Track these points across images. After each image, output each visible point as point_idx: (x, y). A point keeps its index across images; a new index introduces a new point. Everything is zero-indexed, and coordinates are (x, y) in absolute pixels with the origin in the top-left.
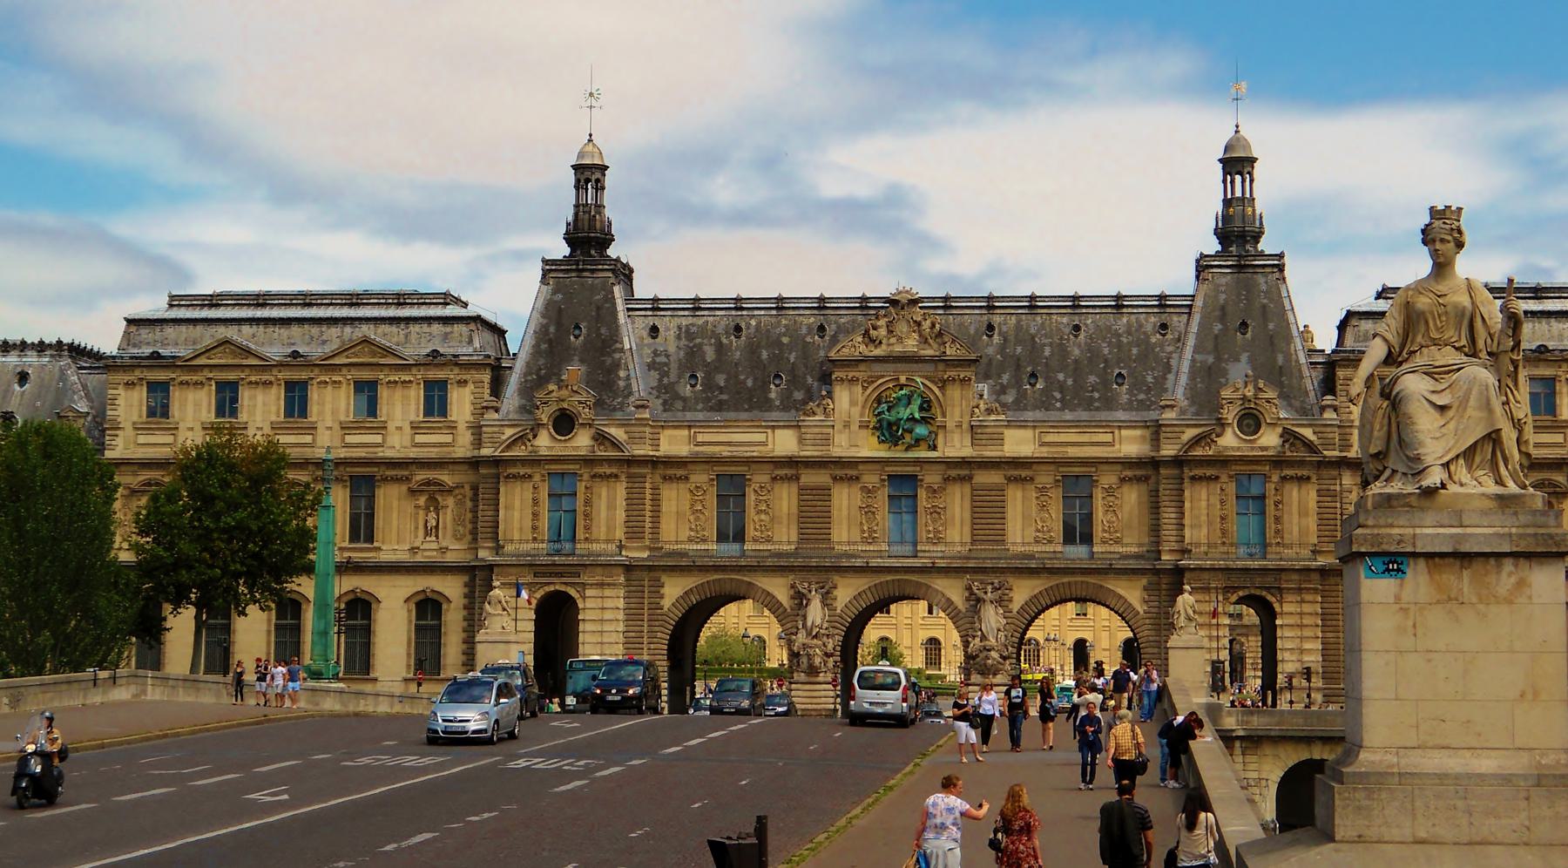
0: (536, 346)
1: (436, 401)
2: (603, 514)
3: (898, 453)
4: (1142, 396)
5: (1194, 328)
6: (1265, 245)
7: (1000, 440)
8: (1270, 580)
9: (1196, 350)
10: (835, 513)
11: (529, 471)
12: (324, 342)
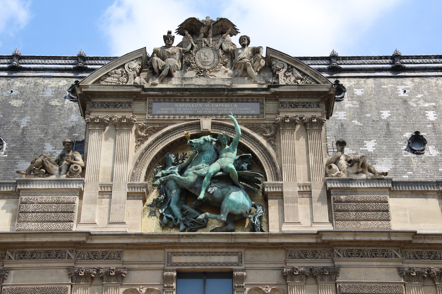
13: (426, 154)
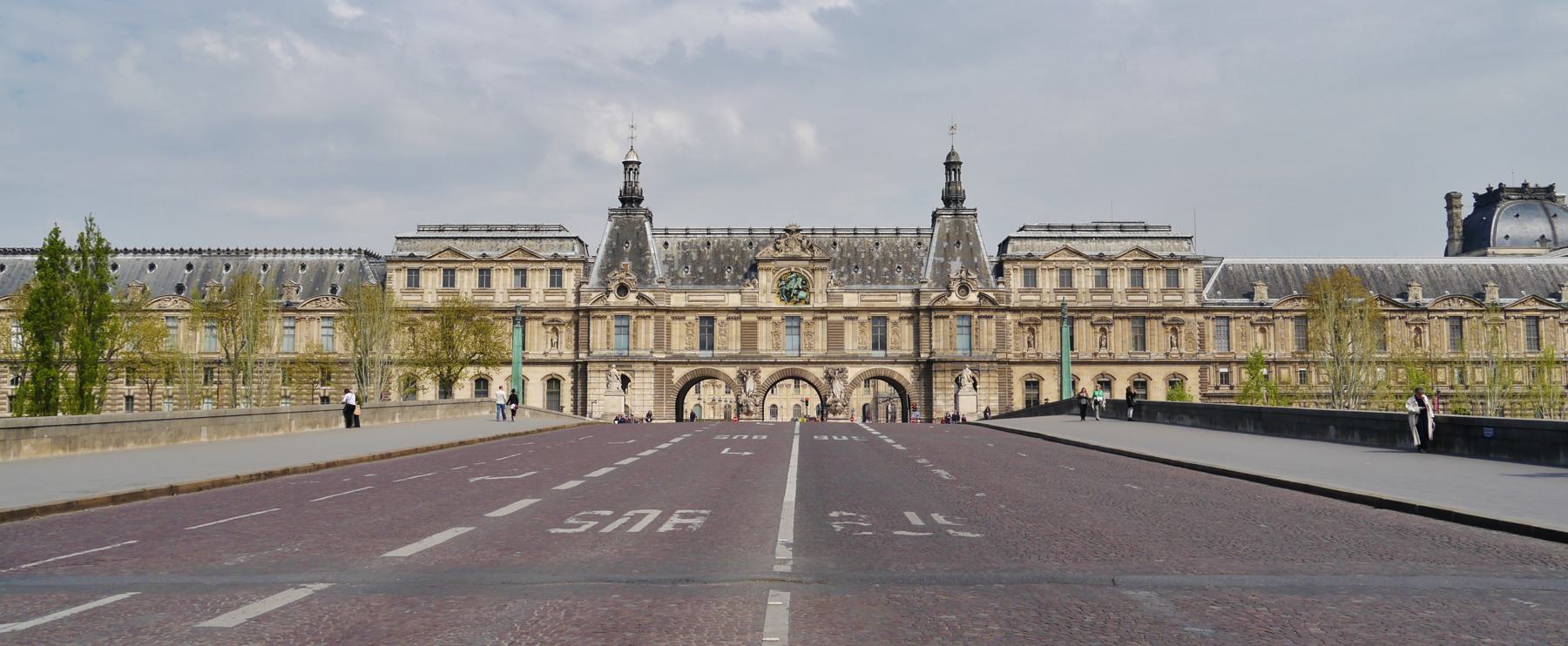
1: (556, 279)
3: (790, 305)
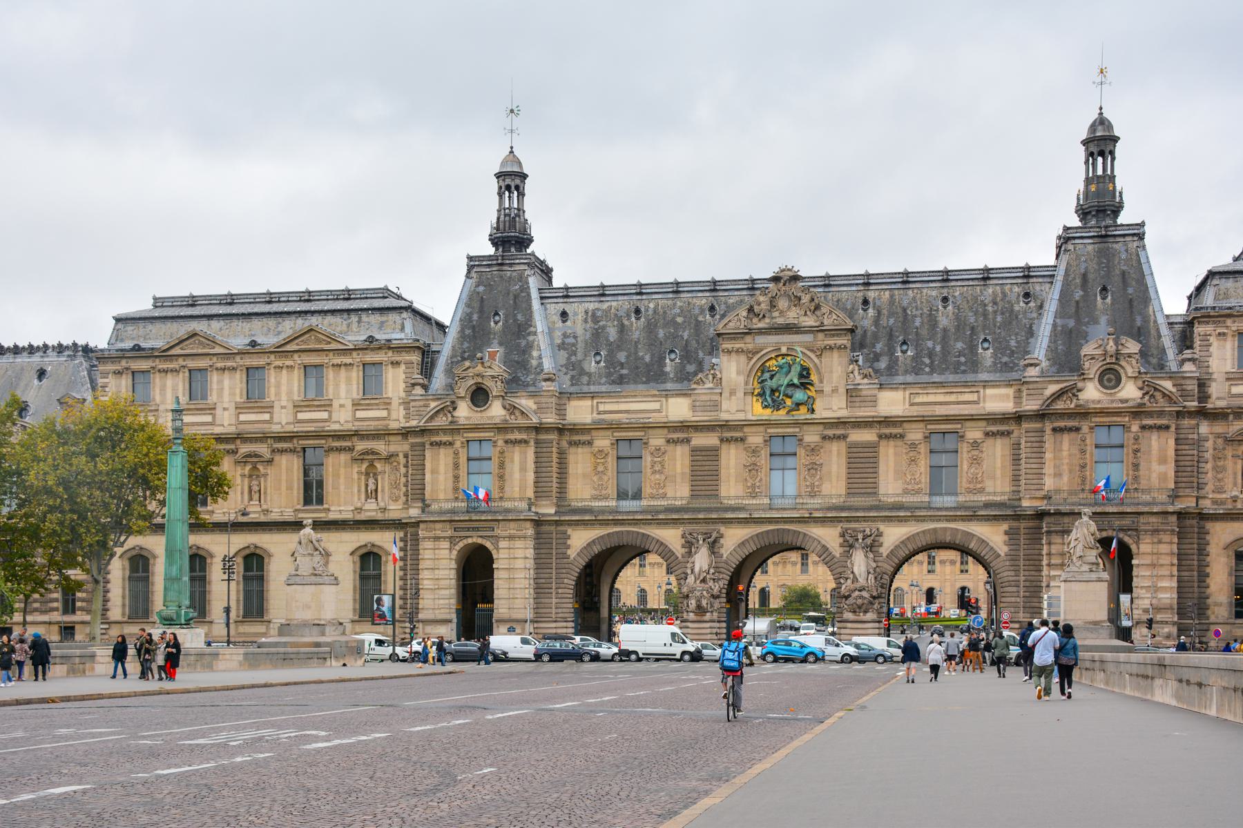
0: (462, 331)
2: (517, 475)
4: (1005, 359)
5: (1056, 296)
6: (1123, 219)
7: (874, 402)
8: (1127, 522)
9: (1057, 315)
10: (723, 472)
11: (450, 439)
12: (279, 333)
13: (909, 353)
